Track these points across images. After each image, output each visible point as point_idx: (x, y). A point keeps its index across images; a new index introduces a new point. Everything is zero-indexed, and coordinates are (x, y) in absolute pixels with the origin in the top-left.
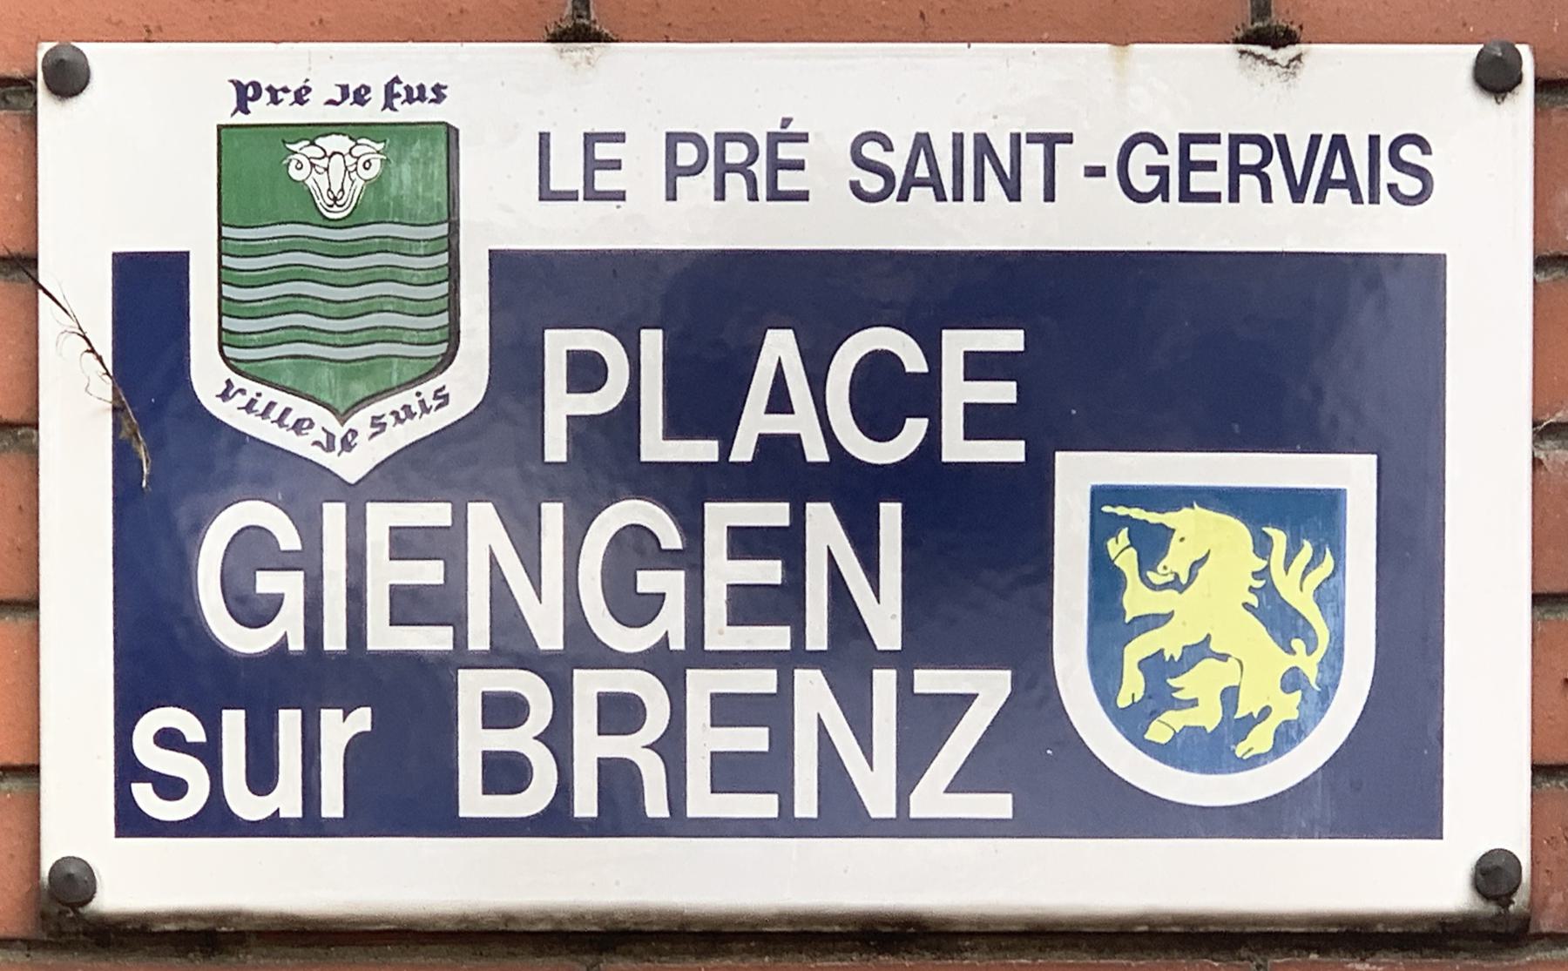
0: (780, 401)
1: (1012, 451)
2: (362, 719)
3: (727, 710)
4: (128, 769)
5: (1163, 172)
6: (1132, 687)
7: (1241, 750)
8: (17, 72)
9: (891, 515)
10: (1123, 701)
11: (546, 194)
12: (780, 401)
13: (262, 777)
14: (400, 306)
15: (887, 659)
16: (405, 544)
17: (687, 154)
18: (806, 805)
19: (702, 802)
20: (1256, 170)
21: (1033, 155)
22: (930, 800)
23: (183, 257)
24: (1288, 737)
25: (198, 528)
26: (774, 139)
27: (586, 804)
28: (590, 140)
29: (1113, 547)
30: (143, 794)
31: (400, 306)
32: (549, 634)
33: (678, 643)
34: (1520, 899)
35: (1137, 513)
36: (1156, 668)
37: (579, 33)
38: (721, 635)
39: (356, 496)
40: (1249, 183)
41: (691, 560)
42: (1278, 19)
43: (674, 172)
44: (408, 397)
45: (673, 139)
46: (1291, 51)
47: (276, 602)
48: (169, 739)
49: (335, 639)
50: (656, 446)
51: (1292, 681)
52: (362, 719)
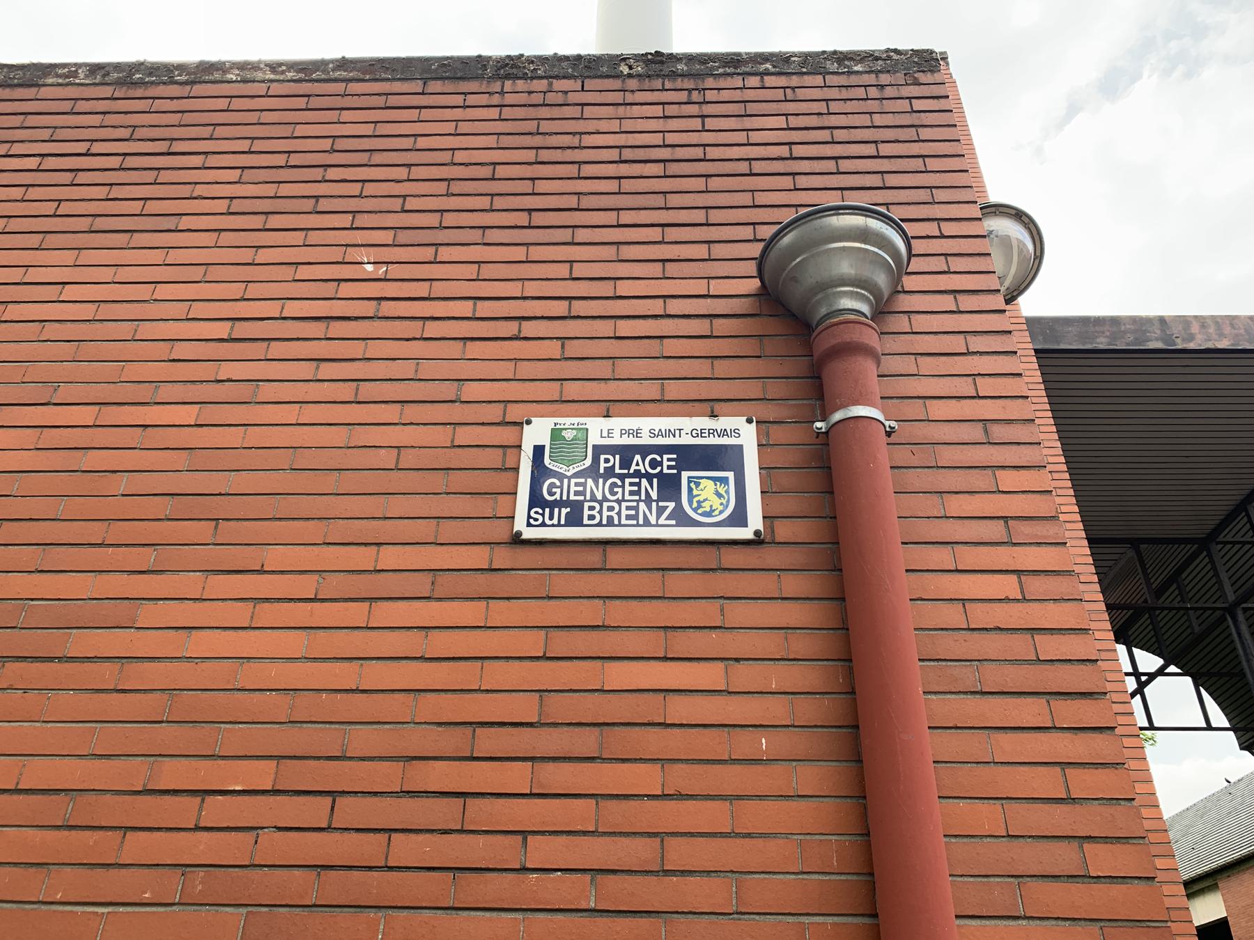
0: (637, 464)
1: (675, 471)
2: (568, 510)
3: (628, 508)
4: (529, 517)
5: (698, 434)
6: (695, 505)
7: (713, 514)
8: (521, 421)
9: (655, 480)
10: (693, 507)
11: (602, 437)
12: (637, 464)
13: (551, 518)
14: (578, 452)
15: (655, 501)
16: (577, 484)
17: (624, 432)
18: (641, 522)
19: (624, 521)
20: (712, 433)
21: (677, 432)
22: (662, 521)
23: (544, 446)
24: (721, 512)
25: (544, 483)
26: (637, 430)
27: (604, 522)
28: (609, 430)
29: (691, 485)
30: (531, 521)
31: (578, 452)
32: (599, 497)
33: (620, 498)
34: (762, 537)
35: (695, 480)
36: (699, 502)
37: (608, 416)
38: (627, 497)
39: (569, 478)
40: (711, 435)
41: (623, 487)
42: (715, 414)
43: (621, 434)
44: (579, 464)
45: (621, 430)
46: (717, 418)
47: (556, 493)
48: (536, 513)
49: (565, 498)
50: (617, 471)
51: (721, 504)
52: (568, 510)
